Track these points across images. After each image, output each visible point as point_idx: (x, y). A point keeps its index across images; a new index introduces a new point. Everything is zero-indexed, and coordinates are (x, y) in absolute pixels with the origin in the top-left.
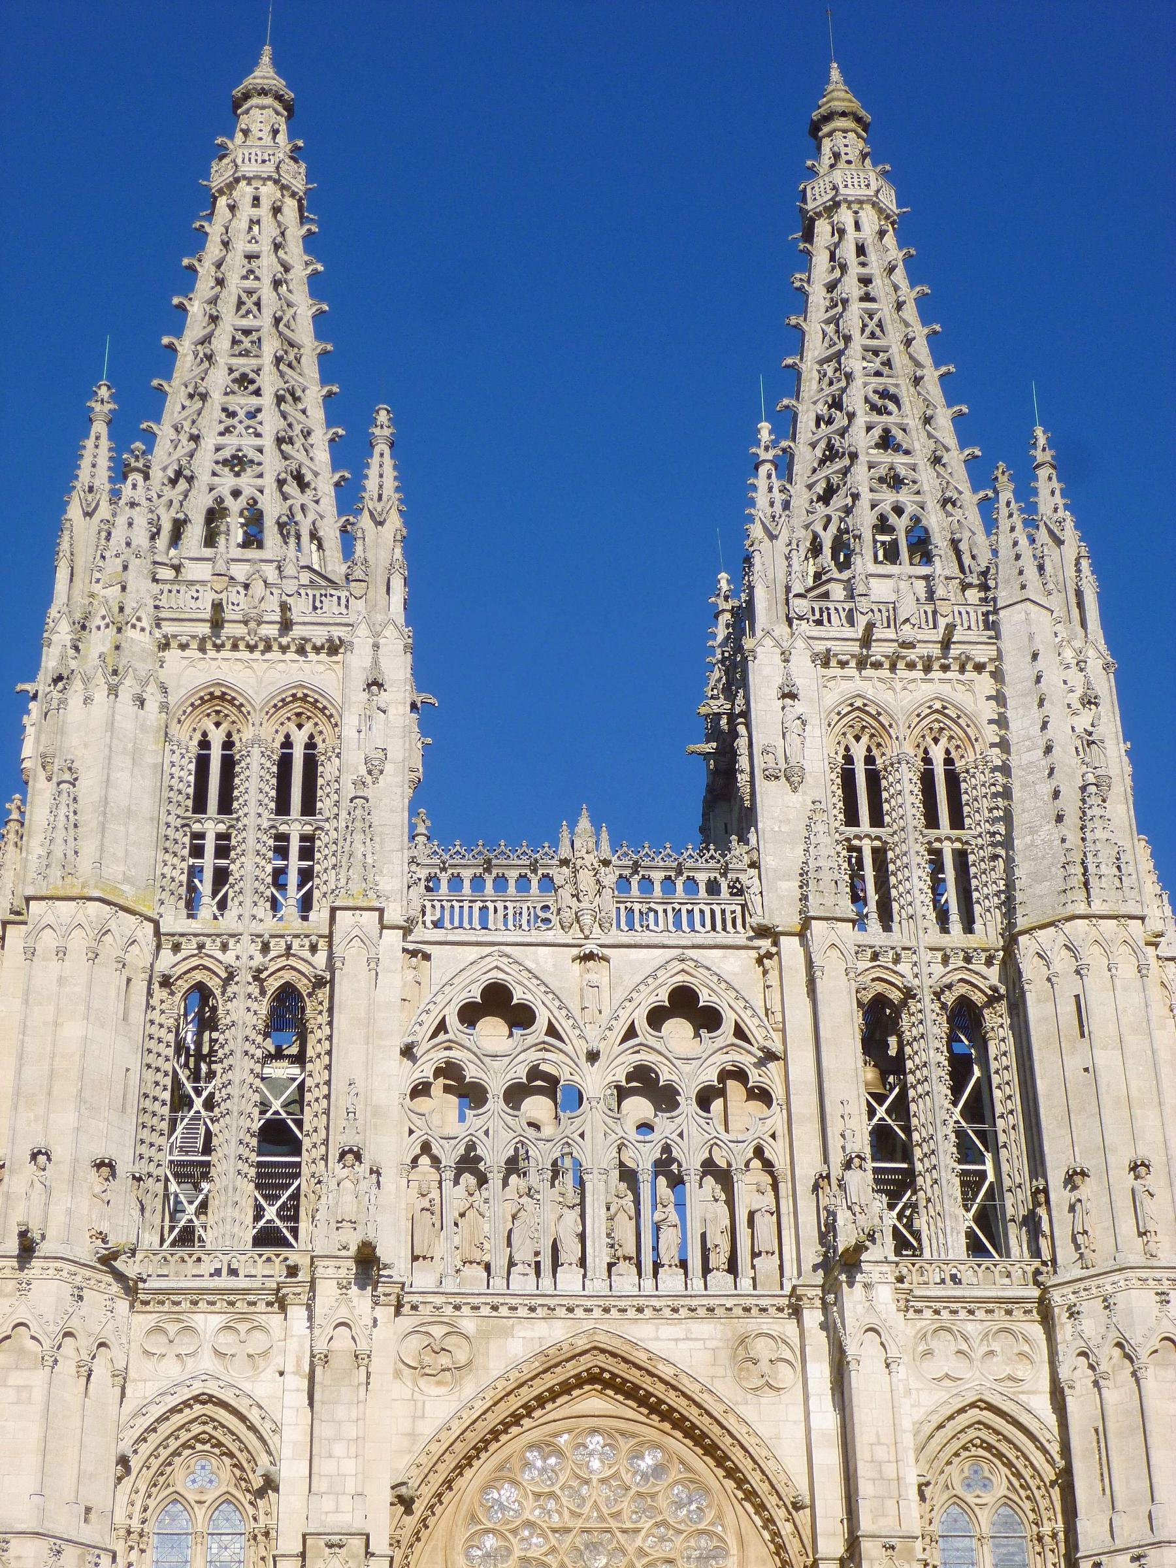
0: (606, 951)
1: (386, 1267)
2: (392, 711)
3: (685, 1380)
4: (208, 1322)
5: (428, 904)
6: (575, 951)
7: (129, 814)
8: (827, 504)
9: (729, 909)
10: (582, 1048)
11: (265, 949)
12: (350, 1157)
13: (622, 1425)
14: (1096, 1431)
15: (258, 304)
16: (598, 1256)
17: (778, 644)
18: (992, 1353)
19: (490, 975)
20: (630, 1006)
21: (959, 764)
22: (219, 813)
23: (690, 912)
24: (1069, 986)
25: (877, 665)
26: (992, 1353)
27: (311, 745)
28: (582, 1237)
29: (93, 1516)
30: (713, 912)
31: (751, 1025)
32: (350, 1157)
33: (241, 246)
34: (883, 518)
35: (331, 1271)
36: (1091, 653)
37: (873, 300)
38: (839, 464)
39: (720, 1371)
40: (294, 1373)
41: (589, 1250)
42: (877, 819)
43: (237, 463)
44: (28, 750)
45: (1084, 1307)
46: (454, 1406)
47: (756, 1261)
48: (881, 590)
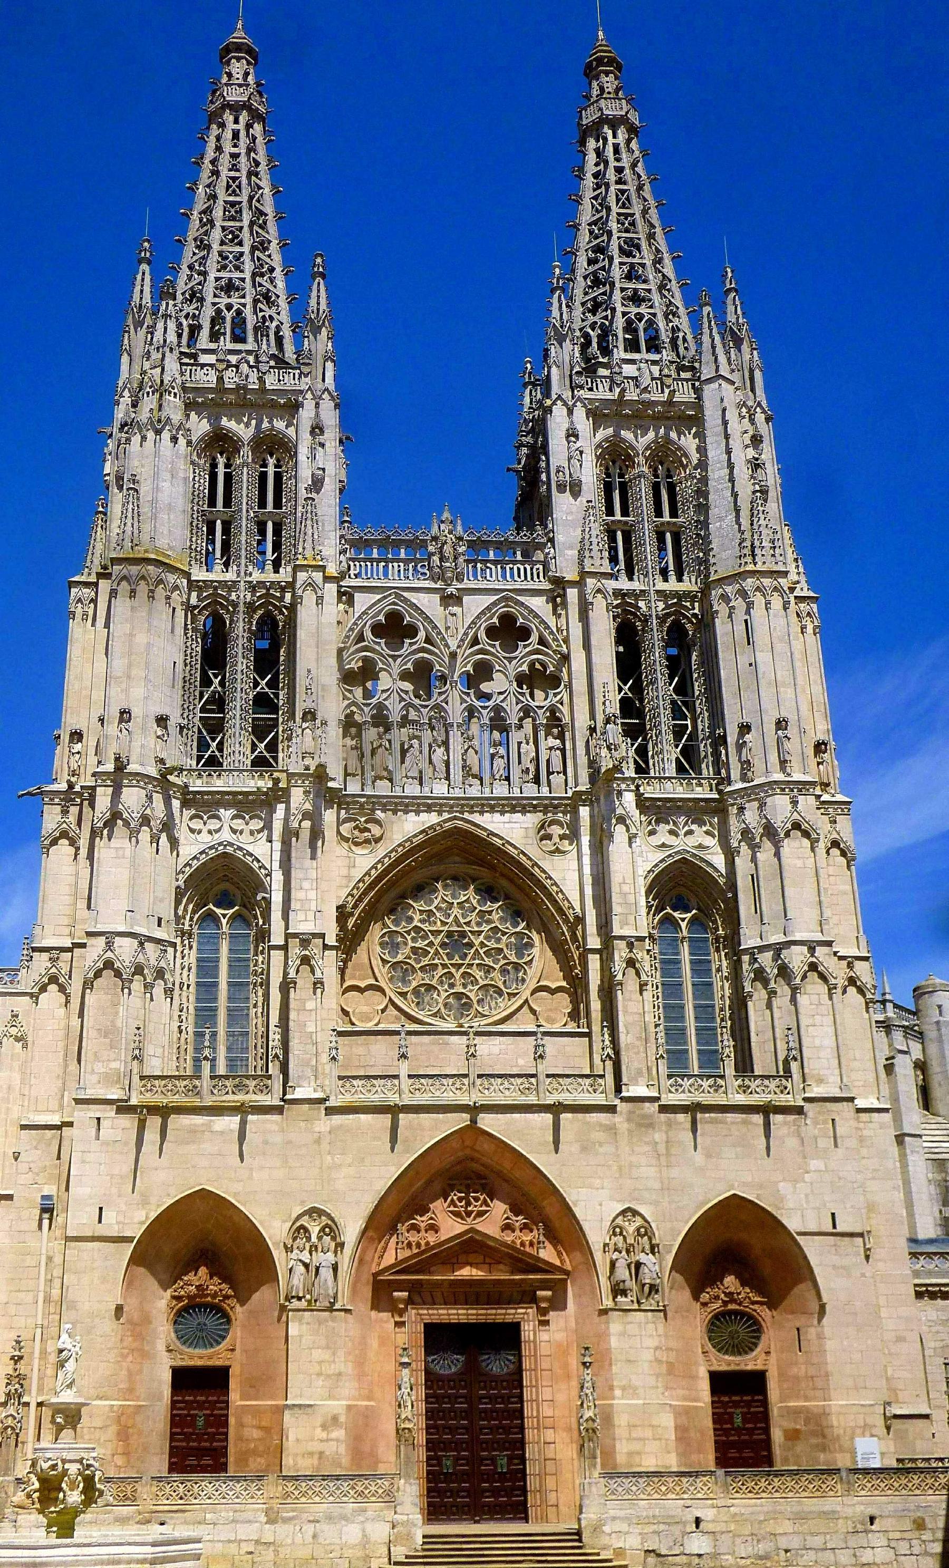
2: (327, 445)
4: (226, 814)
5: (351, 563)
7: (170, 507)
8: (594, 315)
12: (309, 717)
15: (239, 187)
16: (456, 773)
17: (565, 404)
18: (690, 832)
24: (740, 616)
30: (525, 569)
31: (549, 638)
32: (309, 717)
33: (228, 148)
36: (758, 409)
41: (452, 771)
48: (629, 370)
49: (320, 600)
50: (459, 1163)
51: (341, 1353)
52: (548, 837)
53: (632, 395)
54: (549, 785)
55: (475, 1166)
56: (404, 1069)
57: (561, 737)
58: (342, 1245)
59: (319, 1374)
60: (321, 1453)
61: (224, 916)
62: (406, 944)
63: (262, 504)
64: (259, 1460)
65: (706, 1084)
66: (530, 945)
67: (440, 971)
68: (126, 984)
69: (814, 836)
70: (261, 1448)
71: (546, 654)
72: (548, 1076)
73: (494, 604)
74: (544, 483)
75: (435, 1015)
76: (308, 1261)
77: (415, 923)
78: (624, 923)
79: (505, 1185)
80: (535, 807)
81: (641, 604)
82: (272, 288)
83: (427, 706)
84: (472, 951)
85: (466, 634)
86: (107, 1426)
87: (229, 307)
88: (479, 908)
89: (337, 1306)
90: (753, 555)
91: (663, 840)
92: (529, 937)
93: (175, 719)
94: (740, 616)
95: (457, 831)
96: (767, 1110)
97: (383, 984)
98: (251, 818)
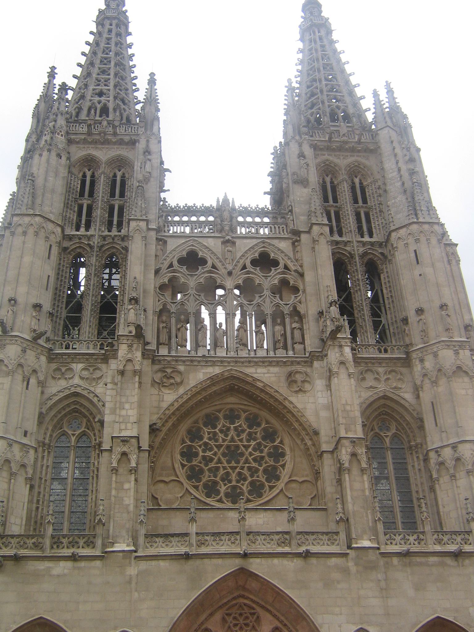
0: (235, 240)
1: (148, 343)
2: (153, 161)
3: (268, 389)
4: (78, 367)
5: (166, 225)
6: (222, 240)
7: (53, 191)
9: (281, 227)
11: (104, 240)
12: (133, 302)
13: (243, 407)
18: (388, 379)
19: (190, 248)
20: (244, 258)
21: (365, 184)
22: (89, 197)
24: (412, 248)
25: (334, 150)
26: (388, 379)
27: (123, 176)
29: (28, 435)
30: (275, 228)
31: (290, 265)
32: (133, 302)
34: (332, 110)
35: (125, 341)
37: (326, 51)
38: (316, 97)
40: (110, 383)
42: (335, 200)
43: (101, 94)
45: (426, 358)
46: (175, 397)
47: (295, 345)
50: (234, 598)
54: (293, 349)
55: (246, 601)
56: (193, 529)
61: (73, 435)
63: (113, 195)
65: (411, 539)
66: (283, 455)
67: (222, 472)
71: (290, 274)
72: (299, 533)
73: (256, 245)
75: (218, 501)
77: (205, 440)
79: (268, 615)
81: (348, 248)
82: (125, 96)
83: (213, 304)
84: (244, 458)
85: (238, 262)
87: (99, 102)
88: (248, 430)
90: (416, 215)
91: (371, 384)
92: (283, 449)
95: (233, 377)
96: (457, 555)
97: (182, 480)
98: (94, 370)
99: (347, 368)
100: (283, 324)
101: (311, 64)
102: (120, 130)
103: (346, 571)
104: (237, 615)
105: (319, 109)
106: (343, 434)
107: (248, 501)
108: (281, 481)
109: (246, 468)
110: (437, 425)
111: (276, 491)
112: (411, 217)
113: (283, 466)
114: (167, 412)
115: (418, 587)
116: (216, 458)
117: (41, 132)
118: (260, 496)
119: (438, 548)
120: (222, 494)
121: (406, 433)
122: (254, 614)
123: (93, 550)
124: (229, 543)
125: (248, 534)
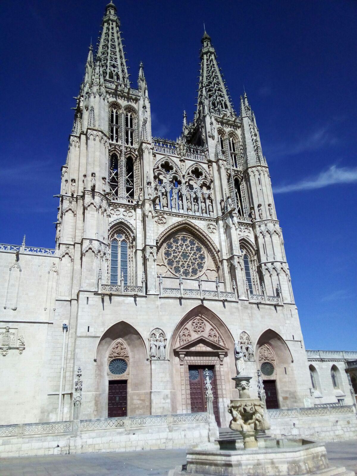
3: (200, 230)
4: (122, 210)
10: (182, 175)
14: (263, 244)
17: (209, 116)
18: (244, 232)
23: (197, 156)
24: (257, 176)
27: (131, 116)
28: (183, 205)
29: (105, 239)
31: (208, 176)
36: (255, 128)
39: (205, 229)
43: (114, 66)
44: (82, 104)
45: (261, 225)
46: (164, 229)
49: (149, 153)
51: (168, 374)
52: (210, 228)
53: (225, 118)
54: (209, 214)
57: (212, 202)
58: (166, 340)
59: (162, 381)
60: (163, 407)
61: (120, 241)
62: (171, 254)
63: (127, 125)
64: (140, 411)
66: (204, 258)
67: (181, 263)
68: (96, 255)
69: (279, 235)
70: (141, 407)
71: (207, 180)
73: (194, 164)
74: (203, 136)
76: (156, 344)
77: (174, 248)
78: (236, 252)
80: (206, 219)
86: (91, 401)
88: (191, 246)
89: (166, 359)
90: (260, 162)
93: (107, 180)
94: (257, 176)
95: (186, 223)
96: (275, 306)
97: (166, 264)
98: (129, 212)
99: (235, 227)
100: (205, 202)
101: (208, 74)
102: (131, 93)
103: (237, 308)
104: (197, 323)
105: (214, 99)
106: (235, 253)
107: (192, 276)
108: (203, 269)
109: (190, 262)
110: (265, 253)
111: (202, 273)
112: (258, 163)
113: (204, 263)
114: (161, 235)
115: (262, 317)
116: (179, 257)
117: (92, 84)
118: (196, 274)
119: (268, 302)
120: (181, 272)
121: (250, 255)
122: (203, 323)
123: (142, 293)
124: (196, 294)
125: (203, 291)
